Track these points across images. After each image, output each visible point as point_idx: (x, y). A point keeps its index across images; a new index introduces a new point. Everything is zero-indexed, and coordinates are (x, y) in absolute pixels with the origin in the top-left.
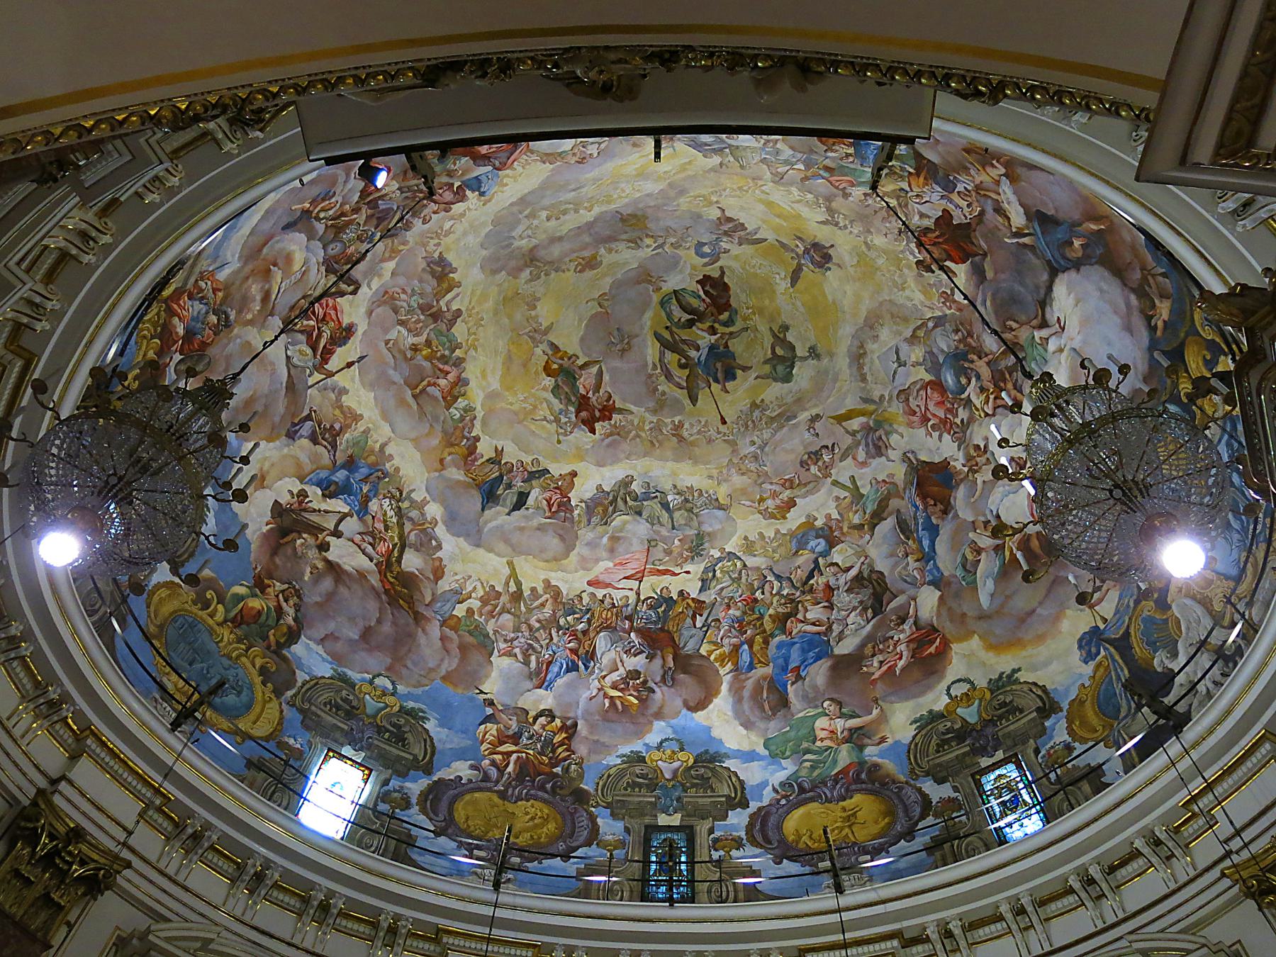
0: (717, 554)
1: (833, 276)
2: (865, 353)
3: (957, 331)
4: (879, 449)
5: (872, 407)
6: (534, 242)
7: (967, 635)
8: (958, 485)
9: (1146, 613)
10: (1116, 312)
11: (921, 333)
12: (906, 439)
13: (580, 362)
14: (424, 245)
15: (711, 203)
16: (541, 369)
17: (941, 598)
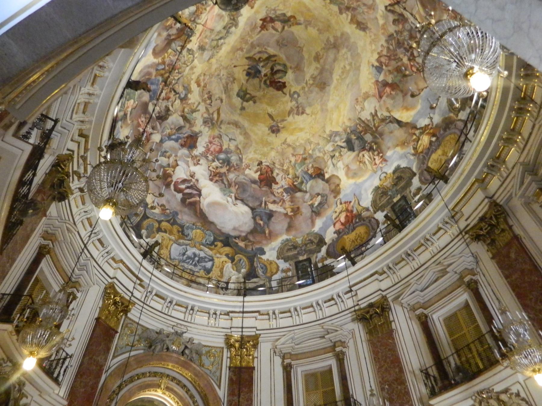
0: (196, 56)
1: (266, 130)
2: (237, 127)
3: (237, 165)
4: (205, 122)
5: (219, 123)
6: (340, 54)
8: (189, 151)
9: (155, 224)
11: (238, 151)
12: (206, 134)
13: (286, 28)
14: (375, 35)
15: (313, 113)
16: (296, 16)
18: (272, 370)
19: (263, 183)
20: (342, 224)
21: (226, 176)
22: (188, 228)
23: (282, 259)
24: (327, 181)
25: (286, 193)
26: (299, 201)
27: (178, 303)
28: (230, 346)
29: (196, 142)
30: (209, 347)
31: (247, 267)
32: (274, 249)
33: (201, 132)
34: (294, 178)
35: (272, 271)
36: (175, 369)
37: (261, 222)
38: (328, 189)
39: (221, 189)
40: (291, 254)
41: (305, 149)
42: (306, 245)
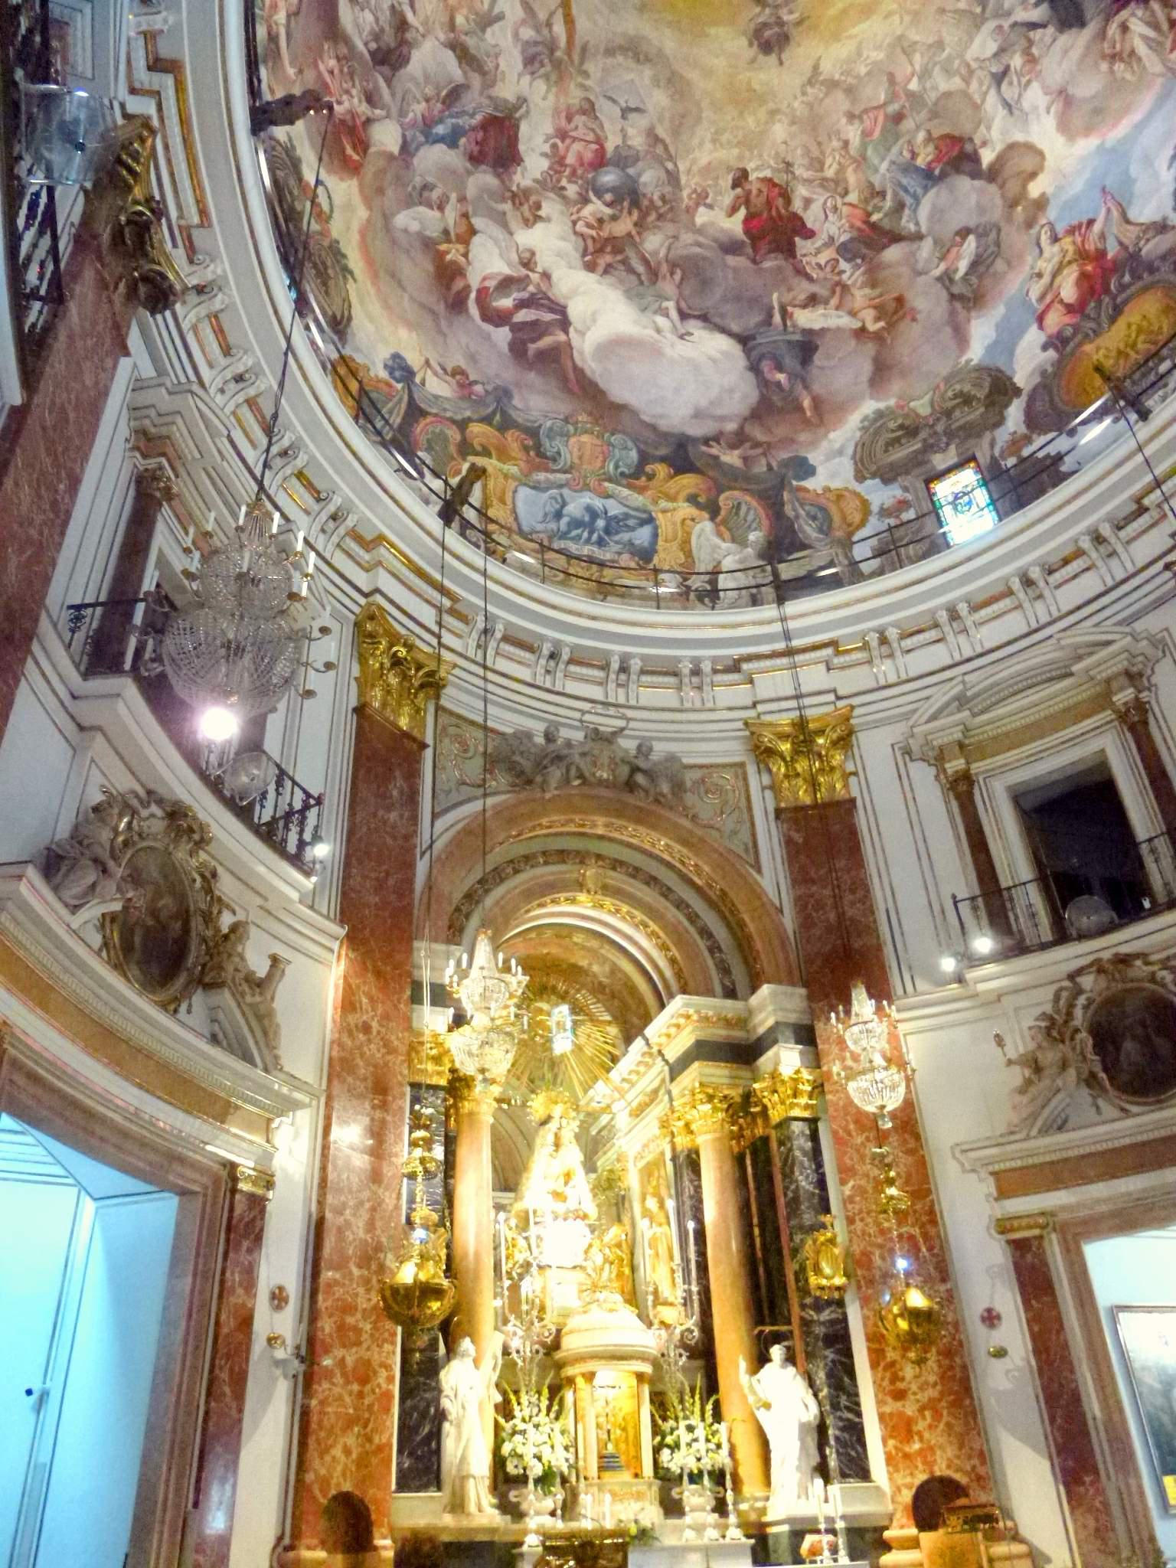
3: (663, 198)
4: (530, 61)
5: (576, 58)
7: (368, 202)
8: (498, 176)
10: (712, 403)
11: (659, 150)
12: (542, 104)
17: (391, 157)
18: (910, 799)
19: (764, 247)
20: (1070, 309)
21: (635, 245)
22: (551, 434)
23: (874, 476)
24: (993, 175)
25: (848, 260)
26: (899, 276)
27: (577, 656)
28: (764, 754)
29: (513, 141)
30: (701, 767)
31: (765, 523)
32: (840, 452)
33: (522, 100)
34: (866, 201)
35: (849, 519)
36: (616, 835)
37: (781, 377)
38: (999, 202)
39: (629, 294)
40: (898, 454)
41: (892, 79)
42: (948, 413)
